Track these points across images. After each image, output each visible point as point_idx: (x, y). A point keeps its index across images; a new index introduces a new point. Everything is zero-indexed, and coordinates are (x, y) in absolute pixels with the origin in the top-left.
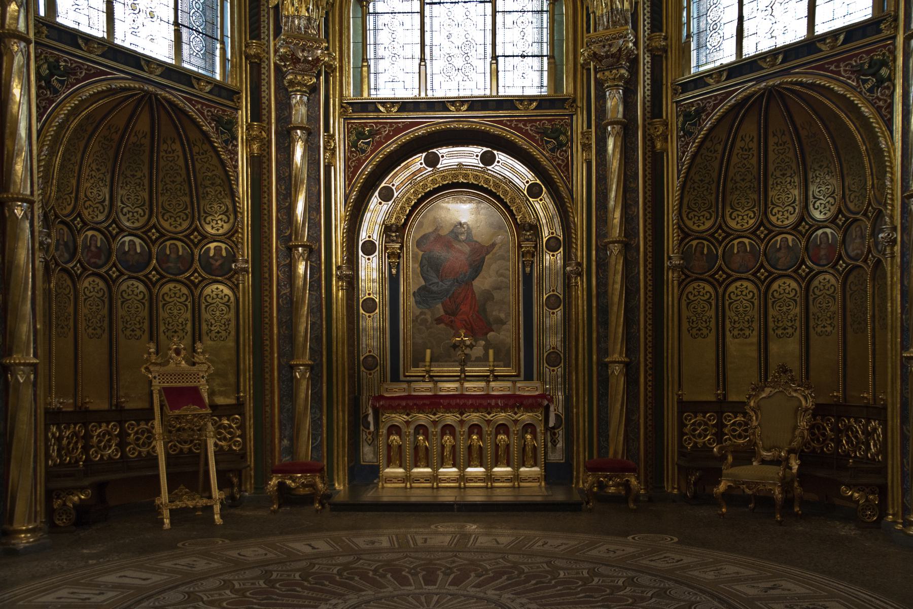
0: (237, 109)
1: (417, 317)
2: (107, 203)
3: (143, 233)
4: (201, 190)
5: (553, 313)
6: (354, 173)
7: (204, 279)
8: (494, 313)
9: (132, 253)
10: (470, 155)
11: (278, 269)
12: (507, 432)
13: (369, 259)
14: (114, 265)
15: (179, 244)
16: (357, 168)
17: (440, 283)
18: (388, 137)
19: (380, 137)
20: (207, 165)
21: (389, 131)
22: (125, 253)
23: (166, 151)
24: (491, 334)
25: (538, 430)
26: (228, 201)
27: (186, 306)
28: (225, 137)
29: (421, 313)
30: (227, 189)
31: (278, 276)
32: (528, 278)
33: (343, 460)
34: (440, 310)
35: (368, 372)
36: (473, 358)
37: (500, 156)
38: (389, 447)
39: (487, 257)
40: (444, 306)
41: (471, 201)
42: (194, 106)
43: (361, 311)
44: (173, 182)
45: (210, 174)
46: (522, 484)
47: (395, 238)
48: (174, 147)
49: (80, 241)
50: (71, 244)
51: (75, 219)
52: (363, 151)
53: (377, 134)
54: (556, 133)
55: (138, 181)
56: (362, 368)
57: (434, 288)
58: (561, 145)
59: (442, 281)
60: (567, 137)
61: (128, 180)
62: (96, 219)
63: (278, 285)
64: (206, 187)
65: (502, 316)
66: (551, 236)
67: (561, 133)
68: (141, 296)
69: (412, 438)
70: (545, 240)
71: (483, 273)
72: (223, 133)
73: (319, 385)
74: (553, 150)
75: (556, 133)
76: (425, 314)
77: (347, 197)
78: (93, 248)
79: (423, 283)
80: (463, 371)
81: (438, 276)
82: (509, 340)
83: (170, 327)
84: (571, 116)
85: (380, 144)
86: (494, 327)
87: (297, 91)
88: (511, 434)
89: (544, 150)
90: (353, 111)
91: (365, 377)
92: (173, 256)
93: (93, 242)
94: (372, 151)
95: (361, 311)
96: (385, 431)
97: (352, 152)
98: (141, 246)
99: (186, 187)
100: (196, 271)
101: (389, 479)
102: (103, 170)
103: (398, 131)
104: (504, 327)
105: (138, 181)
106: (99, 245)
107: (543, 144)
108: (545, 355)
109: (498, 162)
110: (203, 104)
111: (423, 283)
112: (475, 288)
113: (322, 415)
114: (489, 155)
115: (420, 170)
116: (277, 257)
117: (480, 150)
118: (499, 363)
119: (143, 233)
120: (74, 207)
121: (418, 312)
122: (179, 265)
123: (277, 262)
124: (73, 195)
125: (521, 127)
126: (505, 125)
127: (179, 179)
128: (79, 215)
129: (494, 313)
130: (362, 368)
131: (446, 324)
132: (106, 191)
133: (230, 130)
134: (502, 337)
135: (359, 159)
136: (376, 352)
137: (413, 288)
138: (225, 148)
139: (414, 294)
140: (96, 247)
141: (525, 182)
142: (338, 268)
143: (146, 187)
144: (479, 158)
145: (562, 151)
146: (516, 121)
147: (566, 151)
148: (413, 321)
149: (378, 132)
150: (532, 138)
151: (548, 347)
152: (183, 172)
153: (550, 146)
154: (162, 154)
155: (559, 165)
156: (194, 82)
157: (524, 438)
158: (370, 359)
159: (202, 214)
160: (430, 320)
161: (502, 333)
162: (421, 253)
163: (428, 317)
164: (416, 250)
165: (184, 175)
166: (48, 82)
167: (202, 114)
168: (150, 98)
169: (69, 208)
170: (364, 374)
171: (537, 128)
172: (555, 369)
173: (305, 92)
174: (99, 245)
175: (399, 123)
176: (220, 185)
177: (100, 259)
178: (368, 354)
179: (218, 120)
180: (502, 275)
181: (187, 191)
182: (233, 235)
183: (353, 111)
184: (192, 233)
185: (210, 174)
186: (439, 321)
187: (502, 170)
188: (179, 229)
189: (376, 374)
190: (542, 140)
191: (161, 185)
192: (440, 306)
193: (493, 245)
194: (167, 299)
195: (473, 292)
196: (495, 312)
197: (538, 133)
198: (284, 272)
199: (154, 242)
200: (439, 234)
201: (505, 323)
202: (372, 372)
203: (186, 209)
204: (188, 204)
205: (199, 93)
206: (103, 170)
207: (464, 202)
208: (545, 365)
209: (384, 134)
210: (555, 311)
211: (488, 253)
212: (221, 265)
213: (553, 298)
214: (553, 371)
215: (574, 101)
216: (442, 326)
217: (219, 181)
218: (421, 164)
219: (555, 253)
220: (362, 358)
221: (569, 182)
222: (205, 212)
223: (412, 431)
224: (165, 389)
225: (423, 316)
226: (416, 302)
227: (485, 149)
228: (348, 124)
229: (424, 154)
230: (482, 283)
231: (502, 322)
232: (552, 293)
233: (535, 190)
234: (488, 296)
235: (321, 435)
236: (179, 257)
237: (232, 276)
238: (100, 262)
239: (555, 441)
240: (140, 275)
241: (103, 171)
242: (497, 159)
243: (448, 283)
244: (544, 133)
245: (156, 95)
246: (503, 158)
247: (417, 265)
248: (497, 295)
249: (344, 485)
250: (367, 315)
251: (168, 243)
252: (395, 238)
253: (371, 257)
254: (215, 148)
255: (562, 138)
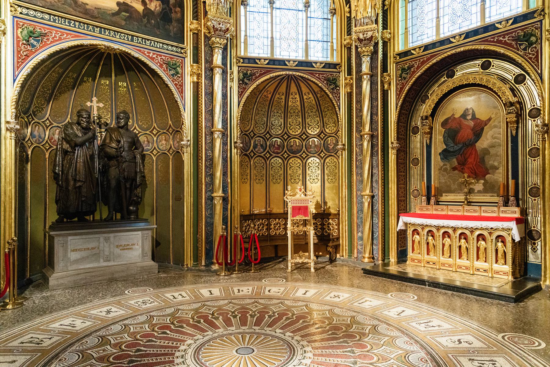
0: (339, 72)
1: (441, 167)
2: (283, 125)
3: (281, 137)
4: (323, 113)
5: (535, 160)
6: (400, 91)
7: (326, 154)
8: (490, 163)
9: (294, 146)
10: (474, 66)
11: (356, 147)
12: (484, 239)
13: (415, 137)
14: (286, 152)
15: (297, 140)
16: (401, 88)
17: (455, 146)
18: (418, 67)
19: (414, 69)
20: (324, 102)
21: (419, 64)
22: (291, 146)
23: (307, 99)
24: (488, 176)
25: (507, 241)
26: (335, 117)
27: (318, 167)
28: (332, 87)
29: (444, 165)
30: (334, 110)
31: (356, 150)
32: (515, 139)
33: (394, 246)
34: (455, 162)
35: (415, 198)
36: (476, 191)
37: (494, 62)
38: (413, 242)
39: (485, 127)
40: (457, 160)
41: (474, 95)
42: (315, 76)
43: (411, 165)
44: (312, 112)
45: (326, 106)
46: (495, 275)
47: (425, 123)
48: (296, 96)
49: (268, 144)
50: (264, 145)
51: (266, 134)
52: (405, 78)
53: (412, 68)
54: (527, 37)
55: (279, 115)
56: (412, 197)
57: (452, 150)
58: (531, 44)
59: (456, 145)
60: (536, 37)
61: (292, 114)
62: (277, 133)
63: (356, 155)
64: (325, 112)
65: (496, 164)
66: (533, 107)
67: (532, 35)
68: (280, 165)
69: (425, 238)
70: (528, 111)
71: (483, 138)
72: (330, 85)
73: (377, 206)
74: (525, 49)
75: (527, 37)
76: (446, 165)
77: (397, 104)
78: (276, 146)
79: (445, 147)
80: (466, 199)
81: (454, 142)
82: (501, 179)
83: (311, 178)
84: (541, 21)
85: (414, 72)
86: (490, 171)
87: (363, 56)
88: (487, 241)
89: (518, 50)
90: (400, 58)
91: (413, 202)
92: (313, 145)
93: (276, 143)
94: (410, 77)
95: (411, 165)
96: (411, 233)
97: (399, 80)
98: (299, 142)
99: (317, 113)
100: (304, 152)
101: (413, 260)
102: (280, 112)
103: (423, 63)
104: (497, 171)
105: (279, 115)
106: (279, 144)
107: (517, 47)
108: (528, 189)
109: (493, 66)
110: (319, 74)
111: (445, 147)
112: (477, 148)
113: (378, 221)
114: (487, 63)
115: (444, 82)
116: (356, 141)
117: (480, 62)
118: (493, 194)
119: (281, 137)
120: (266, 130)
121: (442, 164)
122: (316, 149)
123: (356, 143)
124: (265, 125)
125: (501, 40)
126: (490, 41)
127: (314, 110)
128: (268, 132)
129: (490, 163)
130: (412, 197)
131: (459, 171)
132: (282, 121)
133: (335, 83)
134: (495, 177)
135: (403, 83)
136: (419, 187)
137: (440, 150)
138: (332, 93)
139: (440, 154)
140: (278, 145)
141: (512, 75)
142: (392, 143)
143: (301, 116)
144: (480, 67)
145: (533, 48)
146: (497, 37)
147: (535, 47)
148: (439, 169)
149: (413, 66)
150: (510, 45)
151: (530, 184)
152: (315, 107)
153: (522, 47)
154: (305, 100)
155: (530, 58)
156: (314, 64)
157: (496, 245)
158: (416, 191)
159: (325, 124)
160: (449, 169)
161: (496, 175)
162: (444, 130)
163: (448, 167)
164: (441, 128)
165: (316, 108)
166: (243, 81)
167: (319, 78)
168: (292, 77)
169: (263, 131)
170: (413, 199)
171: (513, 37)
172: (536, 198)
173: (368, 55)
174: (279, 144)
175: (424, 58)
176: (331, 110)
177: (279, 150)
178: (414, 189)
179: (328, 80)
180: (495, 138)
181: (318, 115)
182: (337, 133)
183: (400, 58)
184: (302, 135)
185: (326, 106)
186: (454, 169)
187: (496, 71)
188: (297, 133)
189: (419, 200)
190: (516, 45)
191: (306, 115)
192: (455, 160)
193: (490, 119)
194: (310, 165)
195: (476, 150)
196: (491, 162)
197: (513, 40)
198: (359, 148)
199: (304, 140)
200: (454, 118)
201: (498, 169)
202: (417, 198)
203: (318, 123)
204: (301, 122)
205: (317, 69)
206: (280, 112)
207: (470, 96)
208: (528, 196)
209: (416, 66)
210: (536, 159)
211: (486, 125)
212: (333, 147)
213: (535, 150)
214: (535, 200)
215: (543, 10)
216: (456, 172)
217: (330, 108)
218: (444, 78)
219: (536, 119)
220: (411, 191)
221: (538, 69)
222: (326, 124)
223: (426, 234)
224: (293, 207)
225: (445, 167)
226: (441, 158)
227: (484, 60)
228: (398, 65)
229: (446, 72)
230: (483, 144)
231: (496, 168)
232: (533, 146)
233: (520, 79)
234: (486, 152)
235: (378, 232)
236: (315, 145)
237: (337, 152)
238: (279, 151)
239: (534, 249)
240: (298, 155)
241: (280, 112)
242: (492, 64)
243: (460, 146)
244: (517, 39)
245: (294, 75)
246: (496, 63)
247: (441, 137)
248: (492, 151)
249: (395, 259)
250: (414, 167)
251: (311, 140)
252: (425, 123)
253: (416, 135)
254: (326, 93)
255: (533, 39)
